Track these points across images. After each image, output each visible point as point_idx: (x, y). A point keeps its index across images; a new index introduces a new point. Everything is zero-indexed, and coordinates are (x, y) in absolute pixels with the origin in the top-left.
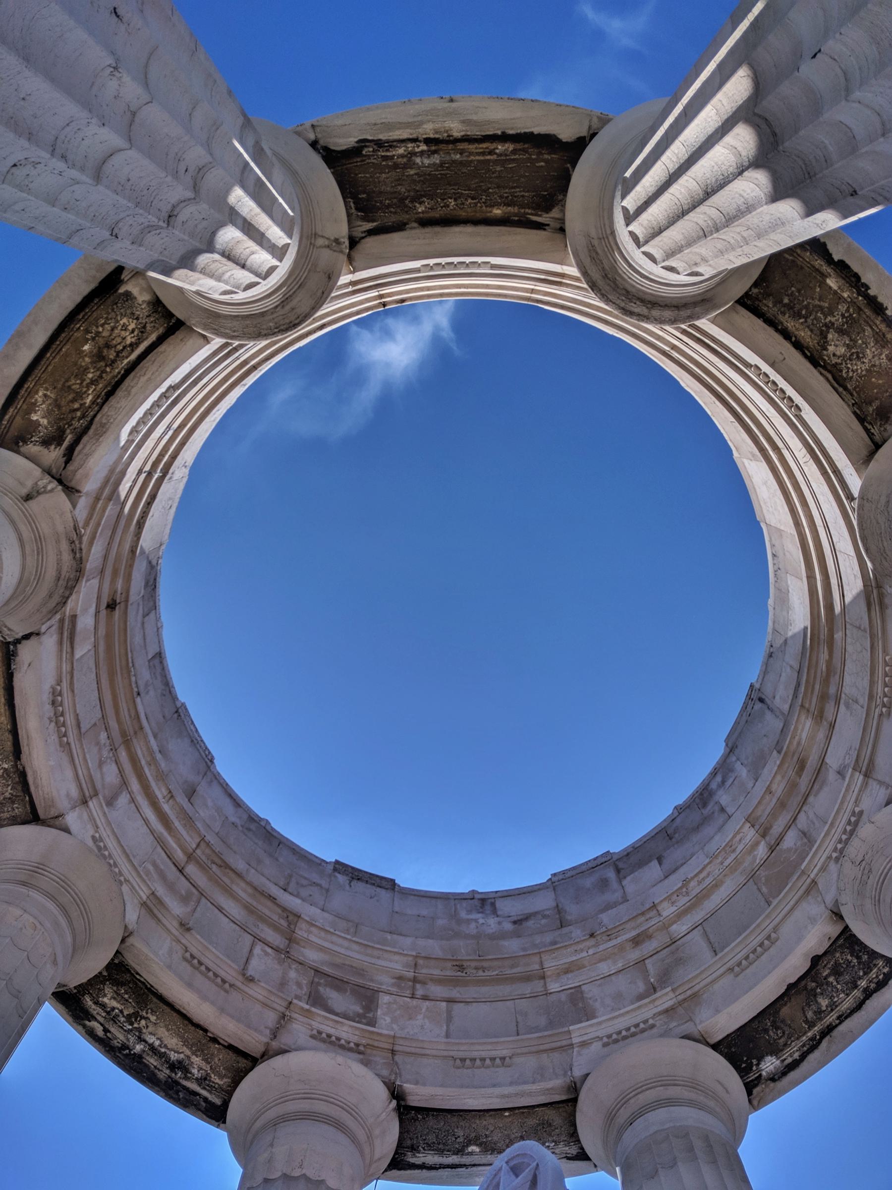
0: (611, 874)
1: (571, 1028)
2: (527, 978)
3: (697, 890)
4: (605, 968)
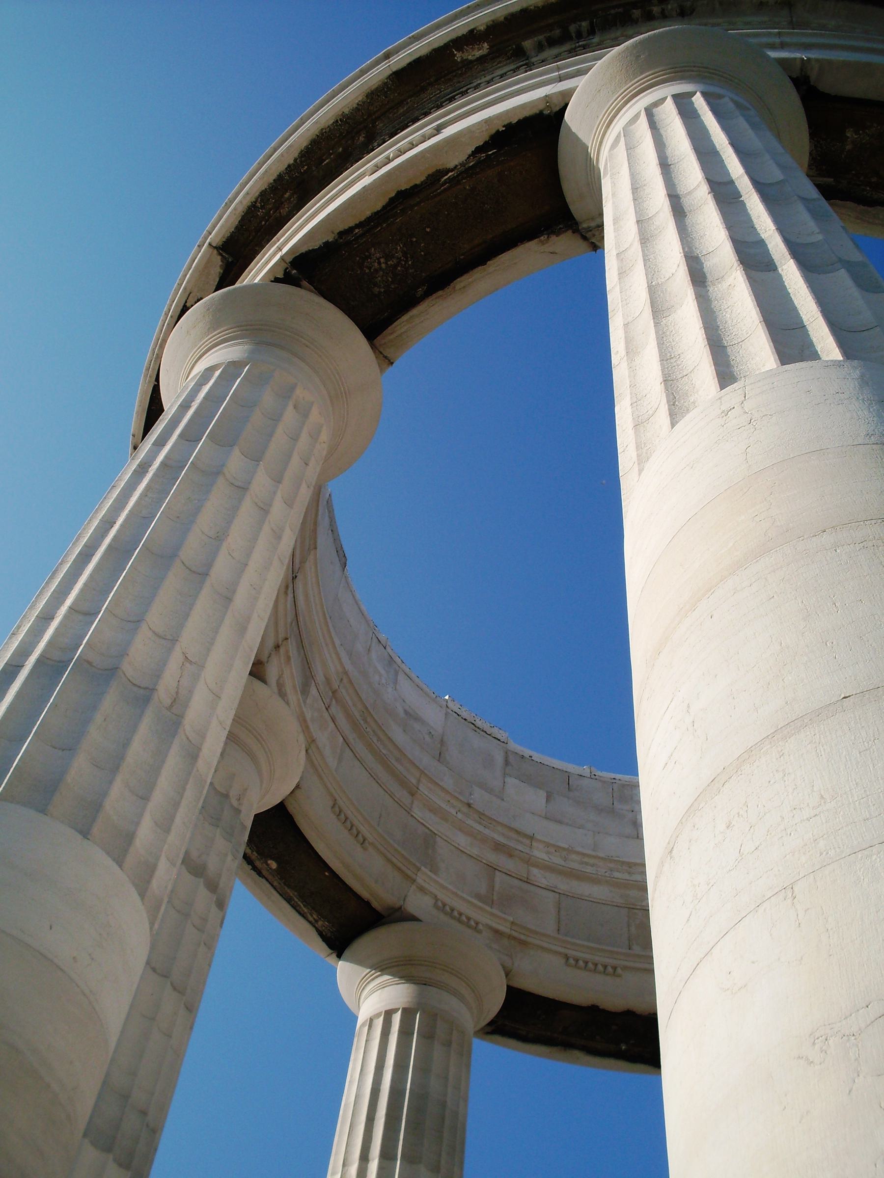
0: (499, 759)
1: (423, 868)
2: (403, 783)
3: (576, 866)
4: (462, 840)
